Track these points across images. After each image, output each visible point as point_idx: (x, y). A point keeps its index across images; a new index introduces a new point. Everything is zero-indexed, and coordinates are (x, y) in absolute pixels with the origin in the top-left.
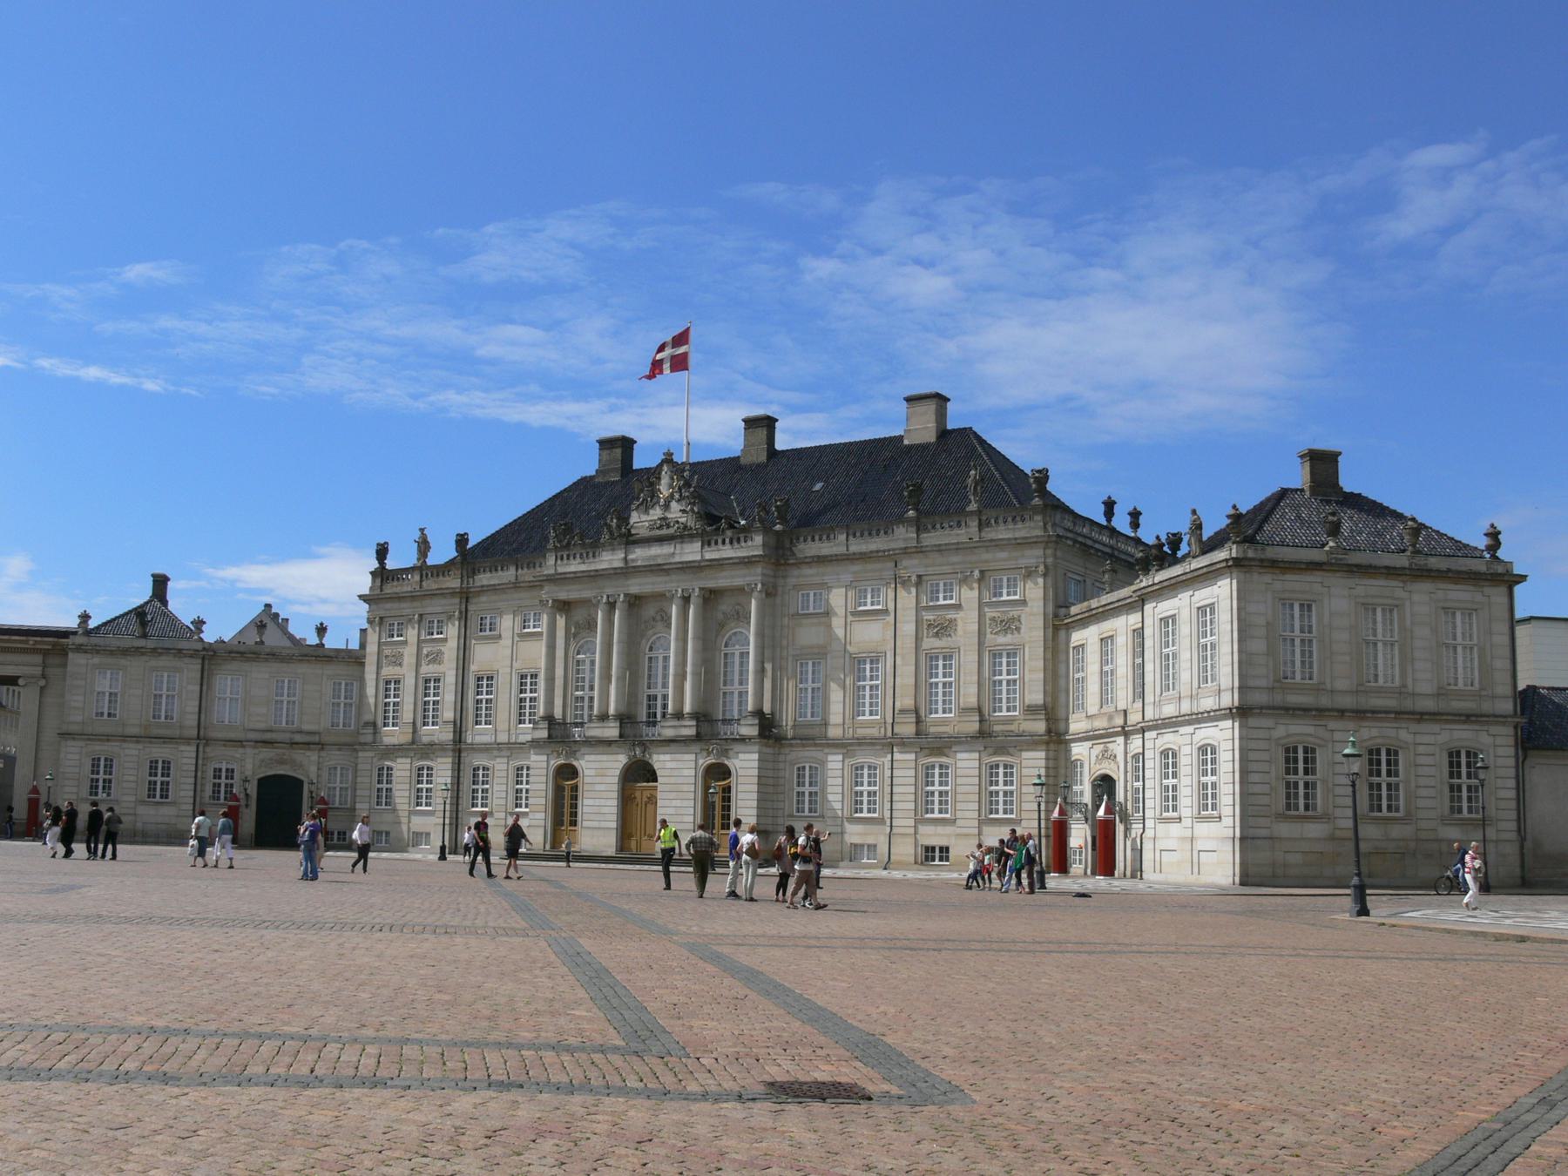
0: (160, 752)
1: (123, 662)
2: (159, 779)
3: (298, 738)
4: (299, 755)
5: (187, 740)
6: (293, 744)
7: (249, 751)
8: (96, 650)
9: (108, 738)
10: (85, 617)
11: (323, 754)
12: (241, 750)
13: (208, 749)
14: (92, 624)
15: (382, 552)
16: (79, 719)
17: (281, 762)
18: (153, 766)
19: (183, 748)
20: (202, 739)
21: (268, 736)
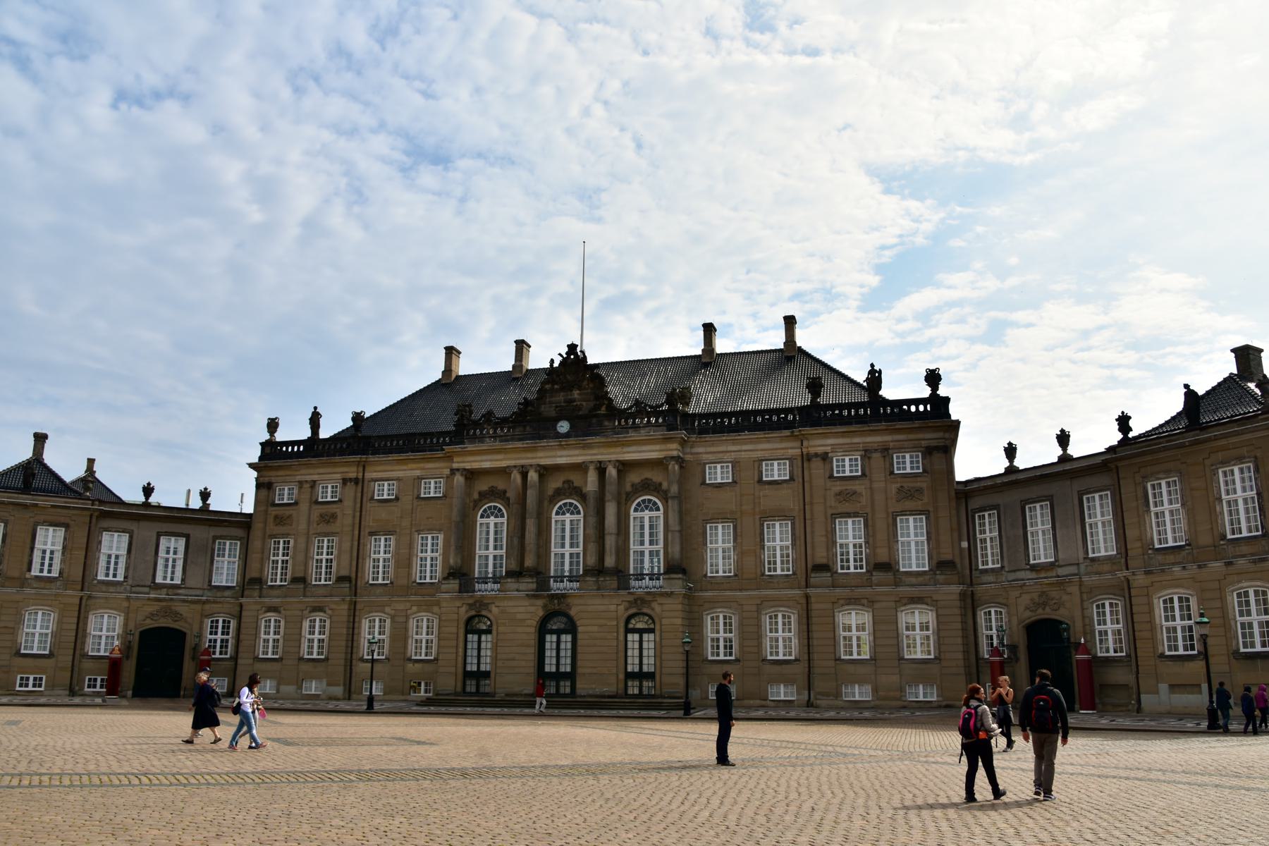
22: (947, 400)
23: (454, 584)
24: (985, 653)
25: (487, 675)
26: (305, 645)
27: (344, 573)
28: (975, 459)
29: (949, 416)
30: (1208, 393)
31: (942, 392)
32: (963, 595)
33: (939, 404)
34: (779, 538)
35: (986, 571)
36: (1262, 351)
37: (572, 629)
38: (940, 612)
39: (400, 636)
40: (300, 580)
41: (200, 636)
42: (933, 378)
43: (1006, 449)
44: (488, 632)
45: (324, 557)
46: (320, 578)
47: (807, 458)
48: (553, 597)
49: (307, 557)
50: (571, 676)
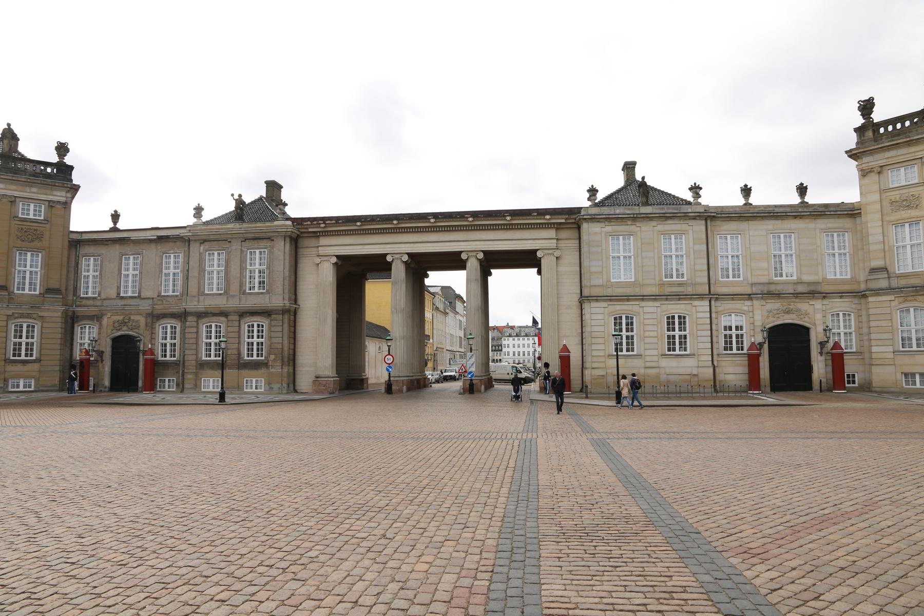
0: (676, 308)
1: (633, 228)
2: (677, 333)
3: (801, 289)
4: (804, 306)
5: (701, 297)
6: (797, 295)
7: (756, 302)
8: (608, 219)
9: (627, 298)
10: (593, 191)
11: (826, 302)
12: (748, 303)
13: (718, 303)
14: (600, 196)
15: (867, 107)
16: (600, 282)
17: (788, 312)
18: (670, 321)
19: (696, 303)
20: (712, 296)
21: (773, 288)
22: (71, 168)
24: (77, 356)
28: (86, 216)
29: (72, 180)
30: (252, 203)
31: (68, 160)
32: (65, 313)
33: (64, 171)
35: (87, 298)
36: (282, 187)
38: (45, 325)
42: (62, 149)
43: (112, 215)
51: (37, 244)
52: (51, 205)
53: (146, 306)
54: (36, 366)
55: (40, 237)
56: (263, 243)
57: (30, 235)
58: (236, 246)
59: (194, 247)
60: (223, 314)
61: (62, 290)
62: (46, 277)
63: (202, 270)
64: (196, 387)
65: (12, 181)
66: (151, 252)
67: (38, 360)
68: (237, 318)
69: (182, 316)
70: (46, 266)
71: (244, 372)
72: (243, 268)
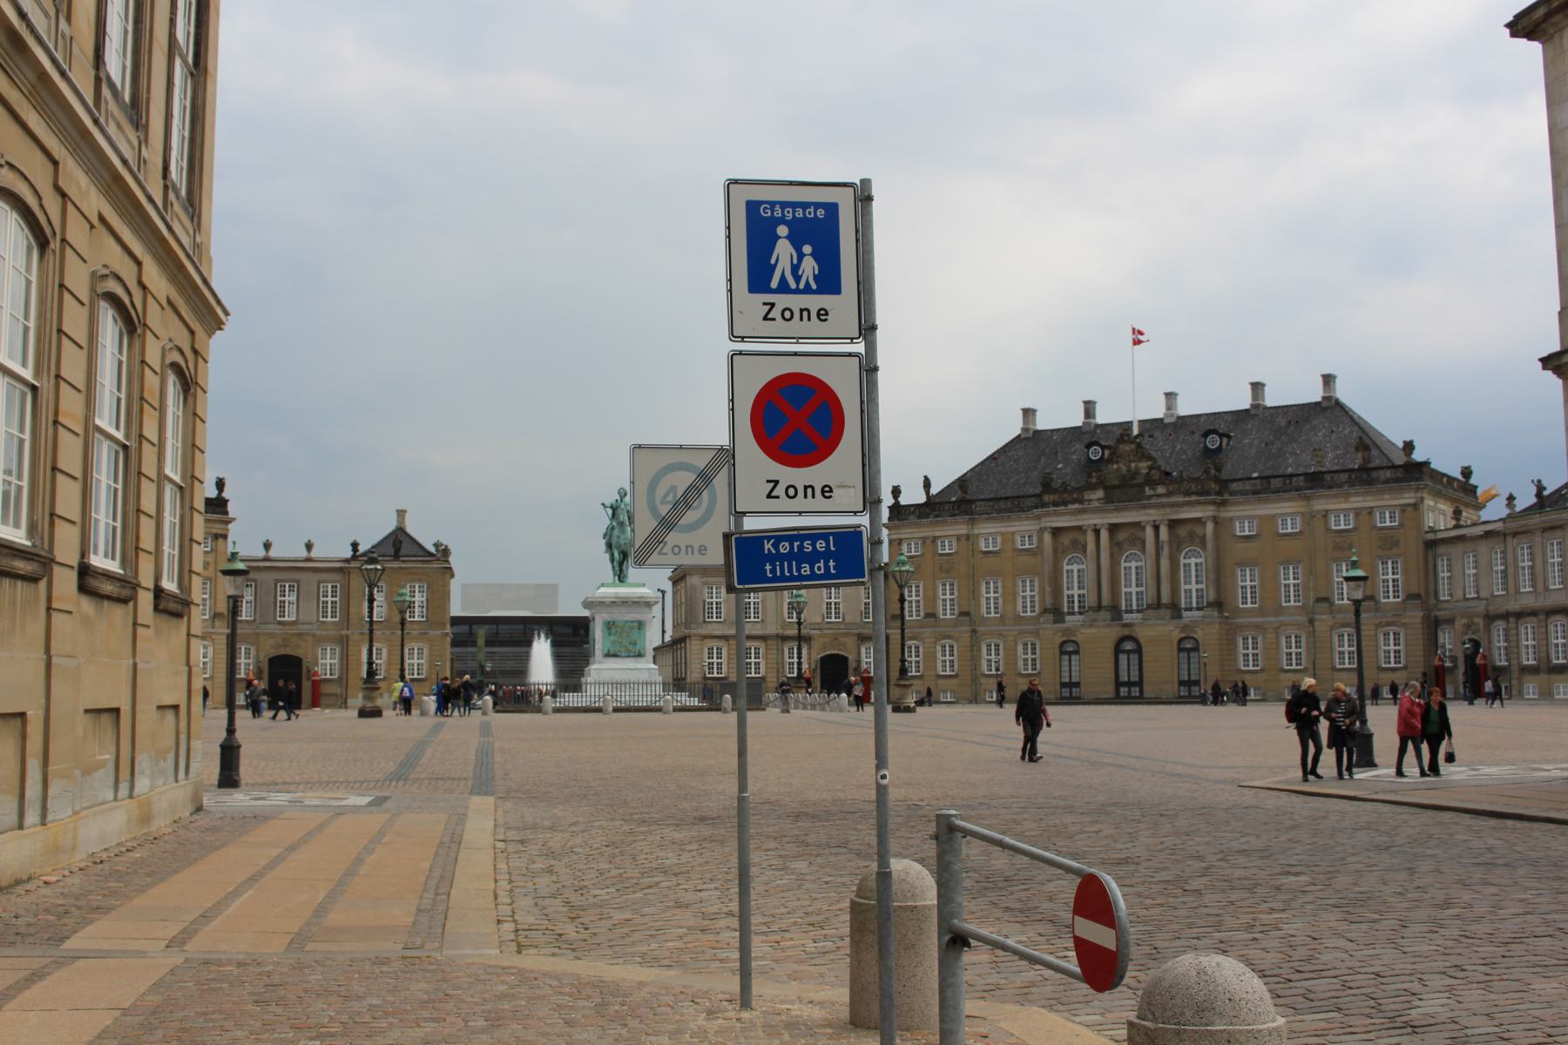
23: (1050, 617)
25: (1077, 685)
26: (940, 664)
27: (965, 609)
32: (1426, 618)
34: (1290, 579)
37: (1139, 650)
39: (1011, 658)
40: (931, 615)
41: (859, 661)
44: (1077, 652)
45: (946, 599)
46: (946, 614)
47: (1313, 516)
48: (1125, 625)
49: (935, 598)
50: (1140, 684)
51: (1395, 550)
52: (1403, 508)
53: (1481, 607)
54: (1404, 673)
55: (1396, 544)
56: (1558, 533)
57: (1388, 543)
58: (1537, 538)
59: (1509, 539)
60: (1533, 613)
61: (1422, 597)
62: (1406, 582)
63: (1516, 566)
64: (1521, 694)
65: (1367, 494)
66: (1483, 547)
67: (1405, 668)
68: (1542, 617)
69: (1505, 616)
70: (1405, 572)
71: (1554, 677)
72: (1545, 562)
